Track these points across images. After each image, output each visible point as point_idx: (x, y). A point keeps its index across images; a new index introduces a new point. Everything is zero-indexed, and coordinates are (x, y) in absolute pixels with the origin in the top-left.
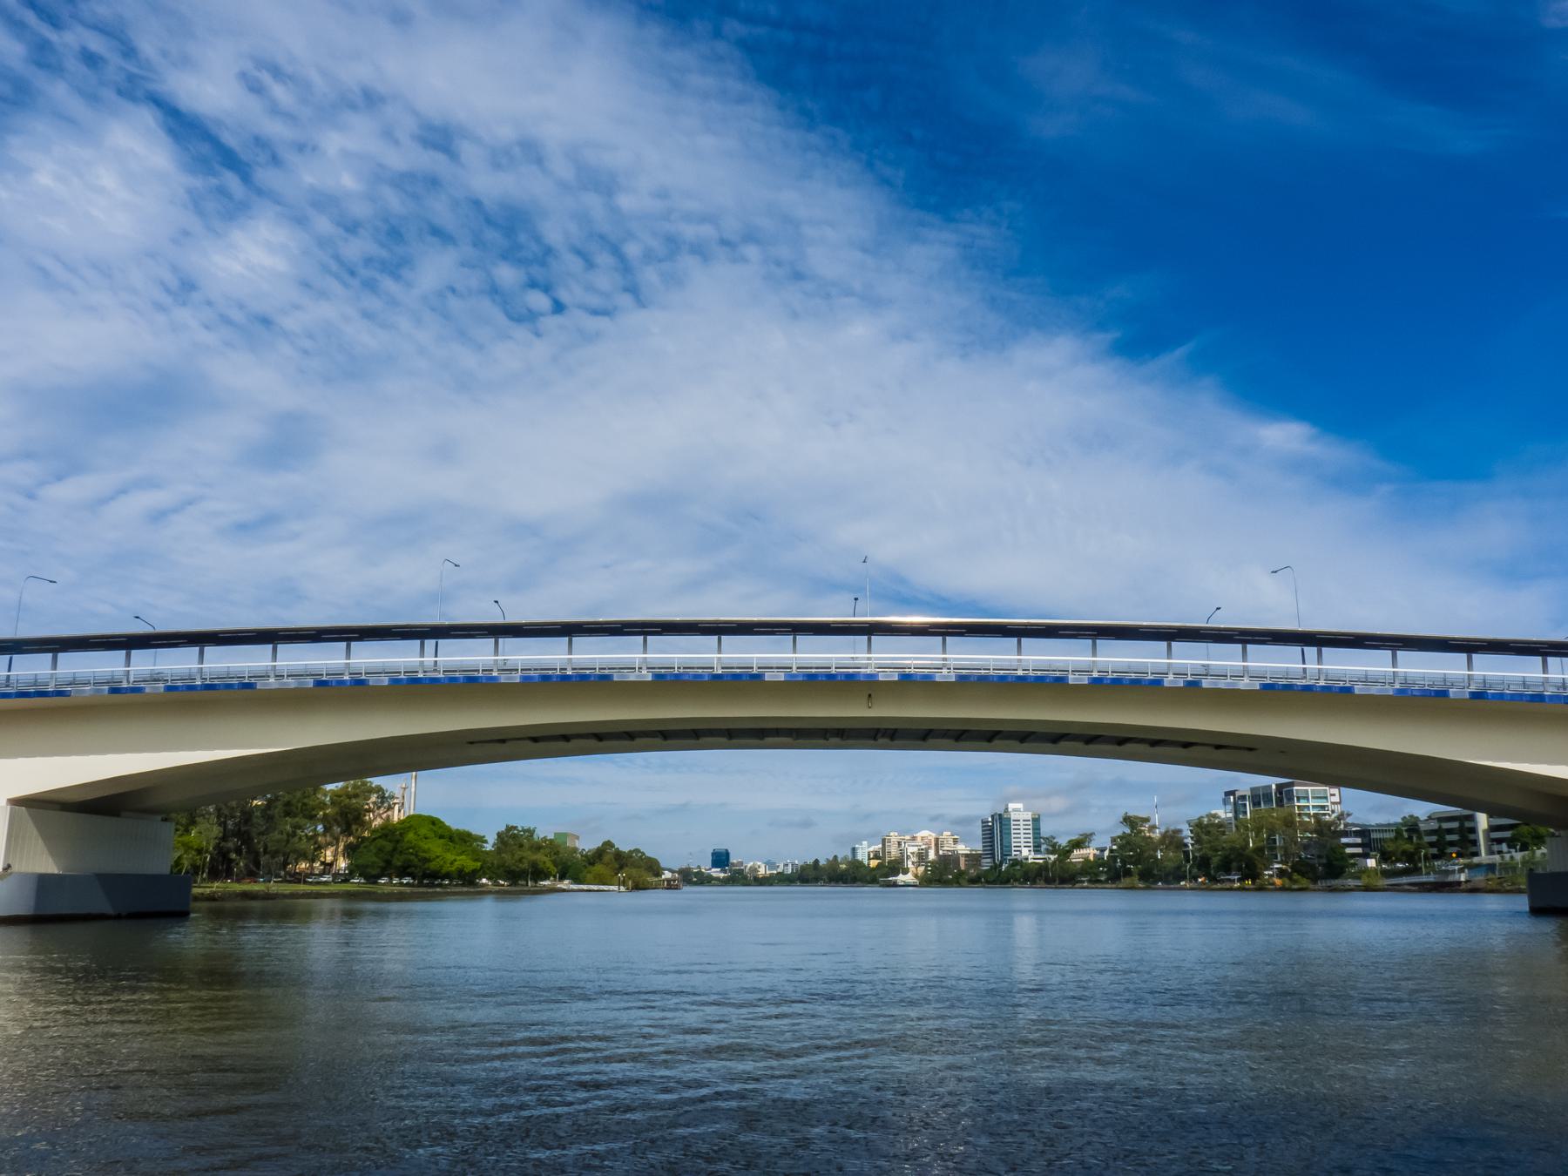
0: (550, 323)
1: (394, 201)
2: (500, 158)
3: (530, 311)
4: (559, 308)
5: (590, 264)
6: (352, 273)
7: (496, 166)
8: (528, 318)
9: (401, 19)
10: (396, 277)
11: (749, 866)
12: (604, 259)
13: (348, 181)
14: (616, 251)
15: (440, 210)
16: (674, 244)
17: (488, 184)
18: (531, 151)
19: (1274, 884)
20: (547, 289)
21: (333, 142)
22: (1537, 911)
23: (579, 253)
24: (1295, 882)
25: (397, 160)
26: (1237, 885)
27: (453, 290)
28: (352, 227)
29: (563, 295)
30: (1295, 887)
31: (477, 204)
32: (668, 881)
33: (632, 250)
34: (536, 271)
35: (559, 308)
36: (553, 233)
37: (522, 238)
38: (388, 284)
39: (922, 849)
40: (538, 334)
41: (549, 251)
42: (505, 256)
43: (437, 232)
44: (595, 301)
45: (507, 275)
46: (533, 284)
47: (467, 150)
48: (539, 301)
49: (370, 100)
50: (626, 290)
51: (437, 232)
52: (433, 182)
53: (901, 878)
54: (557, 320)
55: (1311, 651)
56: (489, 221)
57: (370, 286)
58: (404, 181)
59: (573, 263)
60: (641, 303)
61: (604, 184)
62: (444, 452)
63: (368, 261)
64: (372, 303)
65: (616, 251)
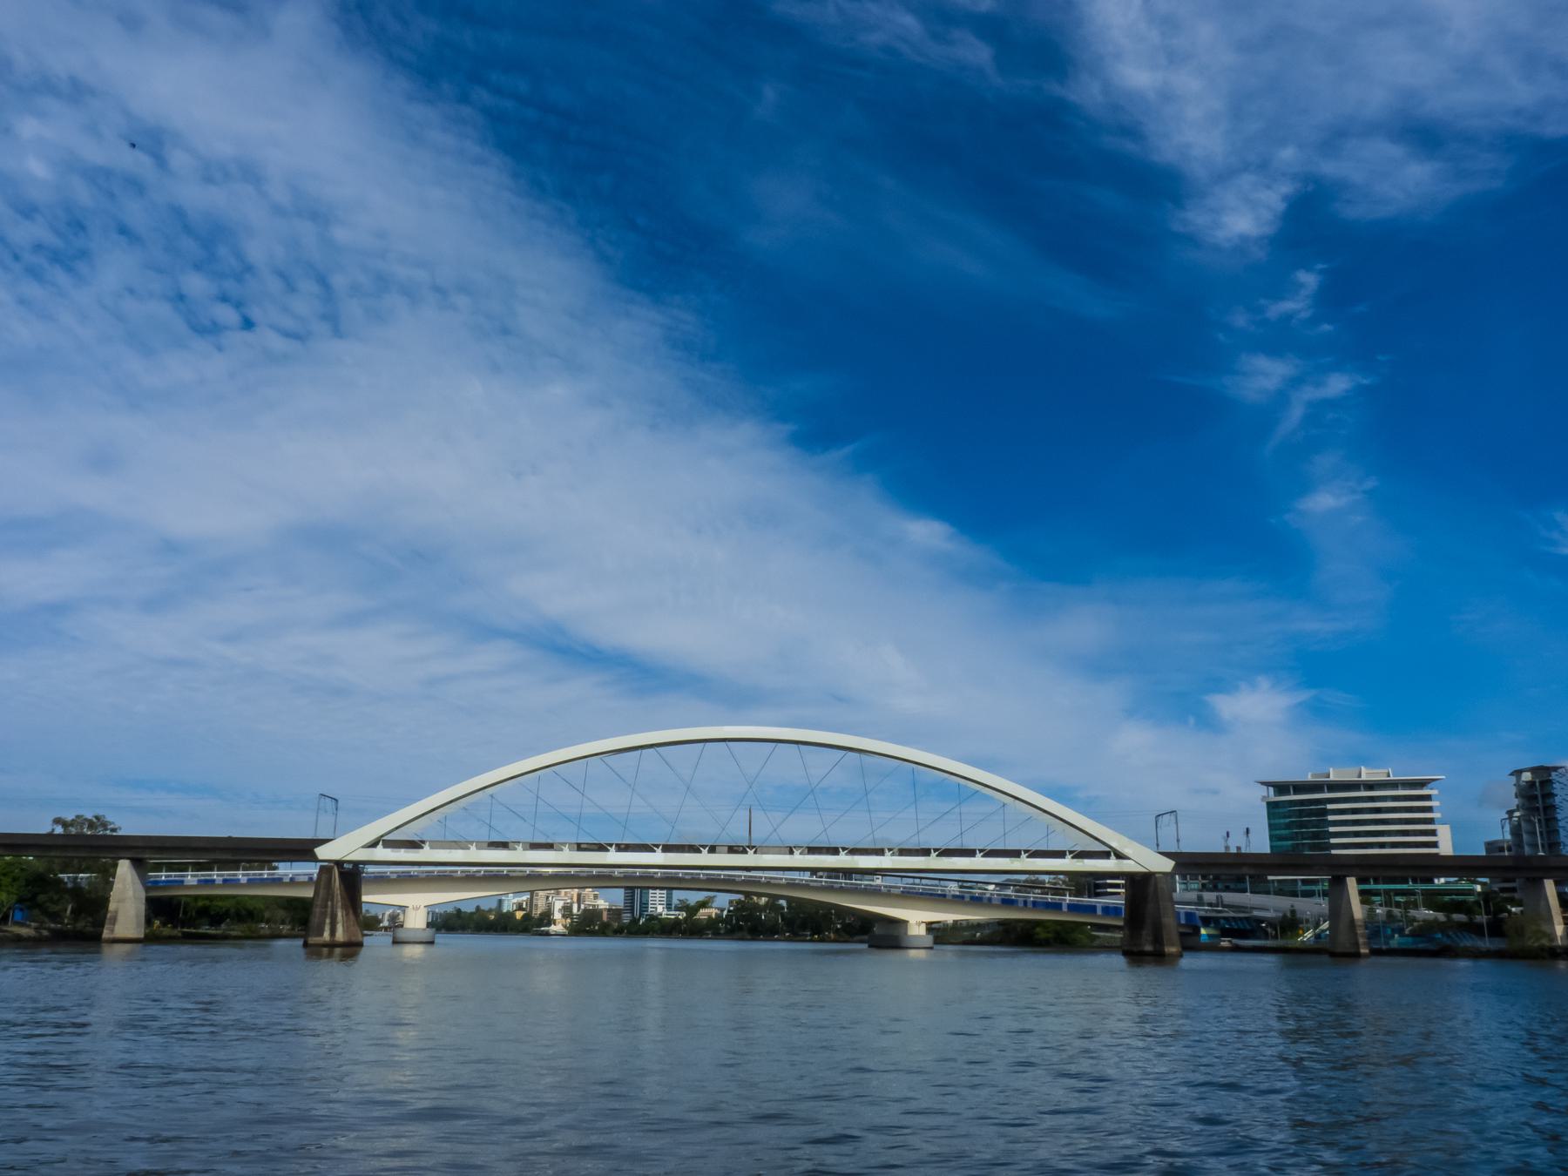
0: (236, 338)
1: (83, 194)
2: (212, 173)
3: (214, 323)
4: (248, 324)
5: (291, 288)
6: (16, 258)
7: (208, 179)
8: (209, 330)
9: (131, 23)
10: (70, 270)
12: (308, 286)
13: (37, 168)
14: (323, 281)
15: (134, 212)
16: (383, 282)
17: (195, 196)
18: (250, 174)
19: (830, 938)
20: (238, 305)
21: (28, 127)
22: (870, 946)
23: (282, 275)
25: (94, 153)
26: (808, 938)
27: (131, 291)
28: (28, 211)
29: (255, 313)
30: (842, 939)
31: (178, 212)
33: (339, 281)
34: (230, 286)
35: (248, 324)
36: (256, 252)
37: (222, 251)
38: (60, 276)
40: (220, 349)
41: (249, 268)
42: (198, 267)
43: (123, 230)
44: (288, 323)
45: (196, 284)
46: (224, 298)
47: (178, 159)
48: (227, 314)
49: (77, 92)
50: (324, 317)
51: (123, 230)
52: (136, 186)
54: (246, 335)
55: (802, 873)
56: (188, 229)
57: (34, 273)
58: (97, 176)
59: (275, 285)
60: (337, 332)
61: (320, 216)
62: (102, 461)
63: (38, 247)
64: (32, 289)
65: (323, 281)
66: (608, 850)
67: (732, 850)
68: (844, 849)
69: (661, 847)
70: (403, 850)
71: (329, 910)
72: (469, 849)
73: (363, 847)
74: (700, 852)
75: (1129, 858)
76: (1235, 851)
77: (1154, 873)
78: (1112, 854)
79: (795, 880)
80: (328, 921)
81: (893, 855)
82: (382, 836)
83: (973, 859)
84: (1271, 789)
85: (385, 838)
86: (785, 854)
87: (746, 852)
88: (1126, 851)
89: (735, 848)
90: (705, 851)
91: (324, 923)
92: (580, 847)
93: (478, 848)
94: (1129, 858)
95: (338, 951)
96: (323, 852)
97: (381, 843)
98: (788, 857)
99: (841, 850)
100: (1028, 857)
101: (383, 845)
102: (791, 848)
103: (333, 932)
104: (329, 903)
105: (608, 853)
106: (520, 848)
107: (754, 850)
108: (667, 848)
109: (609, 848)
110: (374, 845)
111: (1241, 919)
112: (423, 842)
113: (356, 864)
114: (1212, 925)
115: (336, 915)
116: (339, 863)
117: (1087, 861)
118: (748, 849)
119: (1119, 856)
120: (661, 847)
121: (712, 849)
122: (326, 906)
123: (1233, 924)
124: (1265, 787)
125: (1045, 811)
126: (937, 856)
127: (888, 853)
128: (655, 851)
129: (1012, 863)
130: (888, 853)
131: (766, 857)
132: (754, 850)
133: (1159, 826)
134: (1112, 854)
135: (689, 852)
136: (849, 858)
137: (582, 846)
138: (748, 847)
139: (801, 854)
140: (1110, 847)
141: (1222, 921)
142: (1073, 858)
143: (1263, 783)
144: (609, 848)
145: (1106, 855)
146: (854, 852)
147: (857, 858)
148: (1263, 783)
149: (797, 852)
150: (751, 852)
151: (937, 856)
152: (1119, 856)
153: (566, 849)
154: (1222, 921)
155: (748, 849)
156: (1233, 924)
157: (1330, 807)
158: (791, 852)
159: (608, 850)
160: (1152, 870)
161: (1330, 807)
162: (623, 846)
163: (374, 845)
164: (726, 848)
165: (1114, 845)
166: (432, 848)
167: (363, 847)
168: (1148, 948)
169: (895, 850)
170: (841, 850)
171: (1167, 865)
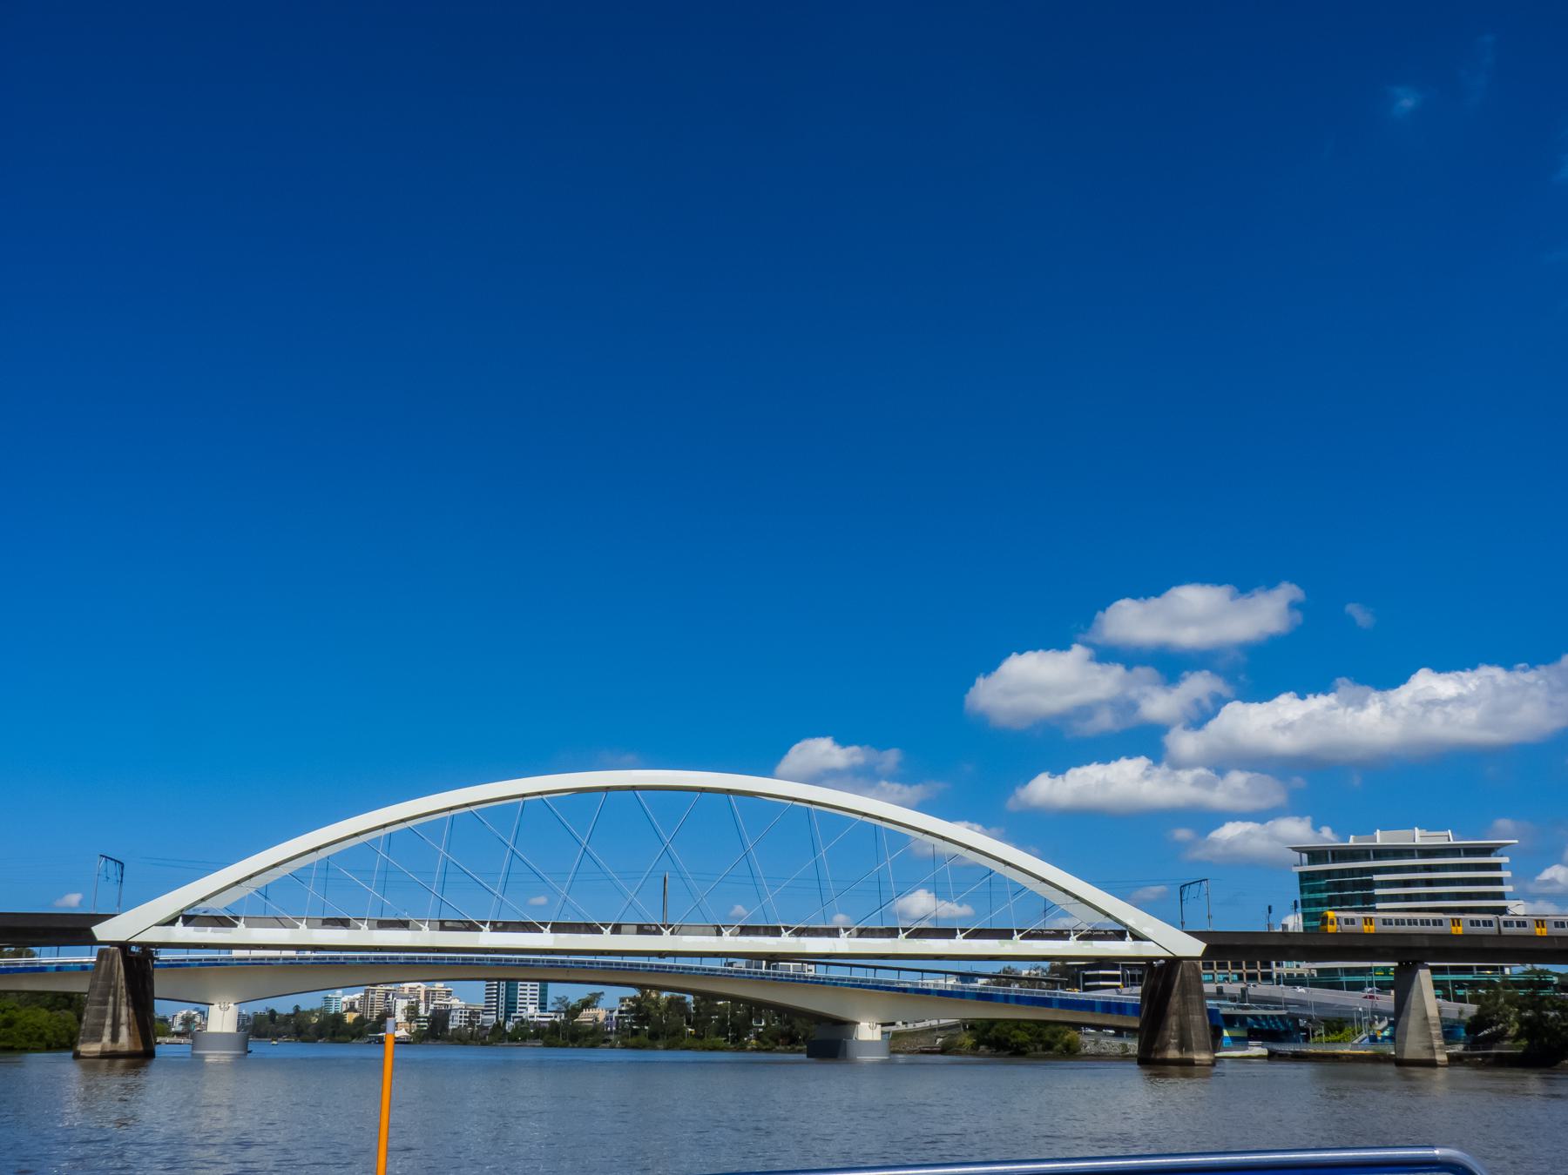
11: (180, 1015)
22: (808, 1056)
24: (765, 1043)
39: (413, 1002)
67: (642, 930)
68: (787, 929)
69: (549, 926)
70: (210, 929)
71: (110, 1008)
72: (297, 927)
73: (156, 925)
74: (601, 932)
75: (1149, 940)
76: (1280, 930)
77: (1180, 959)
78: (1128, 934)
79: (716, 970)
80: (109, 1021)
81: (850, 936)
82: (182, 911)
83: (952, 941)
84: (1305, 856)
85: (185, 913)
86: (710, 934)
87: (661, 933)
88: (1145, 930)
89: (646, 927)
90: (607, 931)
91: (103, 1025)
92: (443, 926)
93: (310, 926)
94: (1149, 940)
95: (121, 1062)
96: (102, 932)
97: (181, 918)
98: (715, 939)
100: (1021, 938)
101: (183, 921)
102: (718, 926)
103: (115, 1037)
104: (111, 999)
105: (481, 933)
106: (364, 926)
108: (557, 928)
110: (171, 922)
111: (1272, 1017)
112: (237, 918)
113: (147, 948)
114: (1237, 1025)
115: (120, 1015)
116: (124, 946)
117: (1096, 943)
118: (663, 929)
119: (1137, 937)
120: (549, 926)
121: (617, 929)
122: (106, 1003)
123: (1264, 1024)
124: (1298, 853)
125: (1044, 880)
126: (907, 937)
127: (843, 934)
128: (541, 931)
129: (1002, 945)
130: (843, 934)
131: (685, 938)
133: (1184, 898)
134: (1128, 934)
136: (794, 940)
137: (447, 924)
138: (663, 926)
139: (731, 935)
140: (1126, 926)
141: (1249, 1020)
142: (1078, 939)
143: (1295, 849)
145: (1120, 935)
146: (800, 932)
147: (804, 940)
148: (1295, 849)
149: (726, 933)
150: (667, 932)
151: (907, 937)
152: (1137, 937)
153: (425, 927)
154: (1249, 1020)
155: (663, 929)
156: (1264, 1024)
157: (1376, 878)
158: (719, 933)
159: (481, 930)
160: (1179, 953)
161: (1376, 878)
162: (499, 925)
163: (171, 922)
164: (635, 928)
165: (1130, 922)
166: (248, 925)
167: (156, 925)
168: (1173, 1054)
169: (854, 931)
171: (1196, 948)
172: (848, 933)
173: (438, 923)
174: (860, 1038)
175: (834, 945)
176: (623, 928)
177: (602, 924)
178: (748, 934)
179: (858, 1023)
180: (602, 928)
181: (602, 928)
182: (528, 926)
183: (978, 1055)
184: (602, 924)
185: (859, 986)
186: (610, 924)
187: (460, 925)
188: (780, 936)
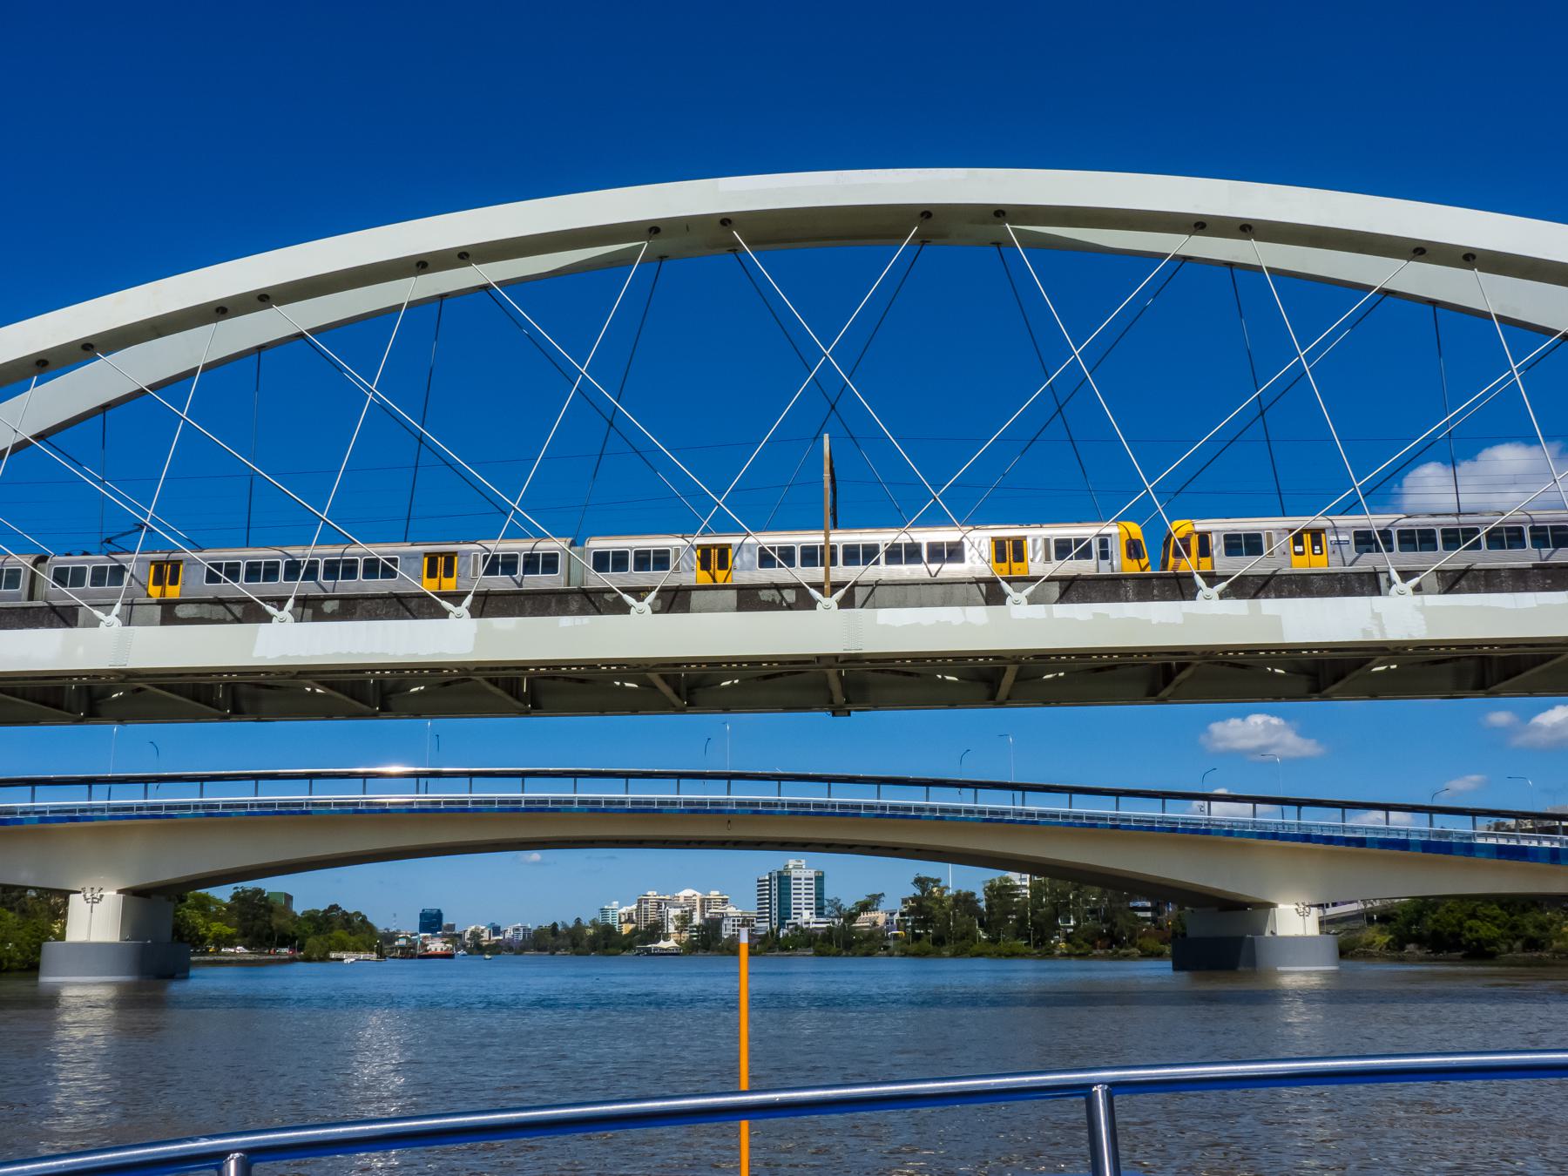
11: (469, 930)
22: (1175, 969)
24: (1079, 947)
32: (402, 948)
39: (686, 912)
53: (662, 944)
55: (1018, 794)
66: (268, 618)
74: (624, 609)
79: (1004, 813)
81: (1418, 589)
87: (811, 604)
89: (765, 595)
98: (980, 614)
99: (1200, 581)
105: (263, 627)
107: (842, 592)
109: (270, 609)
120: (468, 600)
132: (842, 592)
135: (582, 612)
139: (1032, 600)
144: (270, 609)
147: (1270, 606)
164: (732, 595)
170: (1200, 581)
172: (1415, 581)
173: (159, 608)
174: (1280, 932)
175: (1377, 616)
176: (695, 597)
177: (626, 590)
178: (1085, 599)
179: (1273, 905)
180: (626, 597)
181: (626, 597)
182: (413, 604)
183: (1401, 960)
184: (626, 590)
185: (1275, 836)
186: (653, 589)
187: (206, 610)
188: (1193, 597)
